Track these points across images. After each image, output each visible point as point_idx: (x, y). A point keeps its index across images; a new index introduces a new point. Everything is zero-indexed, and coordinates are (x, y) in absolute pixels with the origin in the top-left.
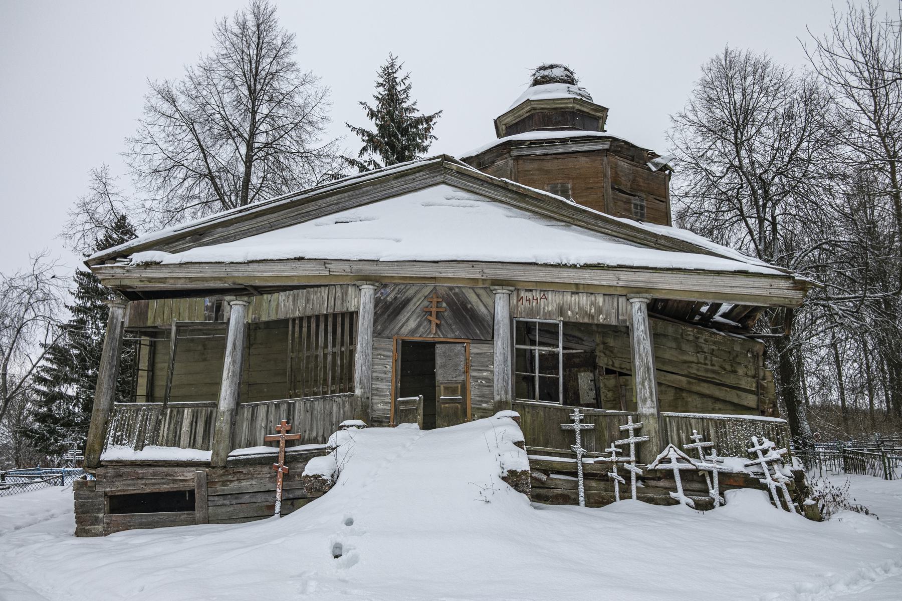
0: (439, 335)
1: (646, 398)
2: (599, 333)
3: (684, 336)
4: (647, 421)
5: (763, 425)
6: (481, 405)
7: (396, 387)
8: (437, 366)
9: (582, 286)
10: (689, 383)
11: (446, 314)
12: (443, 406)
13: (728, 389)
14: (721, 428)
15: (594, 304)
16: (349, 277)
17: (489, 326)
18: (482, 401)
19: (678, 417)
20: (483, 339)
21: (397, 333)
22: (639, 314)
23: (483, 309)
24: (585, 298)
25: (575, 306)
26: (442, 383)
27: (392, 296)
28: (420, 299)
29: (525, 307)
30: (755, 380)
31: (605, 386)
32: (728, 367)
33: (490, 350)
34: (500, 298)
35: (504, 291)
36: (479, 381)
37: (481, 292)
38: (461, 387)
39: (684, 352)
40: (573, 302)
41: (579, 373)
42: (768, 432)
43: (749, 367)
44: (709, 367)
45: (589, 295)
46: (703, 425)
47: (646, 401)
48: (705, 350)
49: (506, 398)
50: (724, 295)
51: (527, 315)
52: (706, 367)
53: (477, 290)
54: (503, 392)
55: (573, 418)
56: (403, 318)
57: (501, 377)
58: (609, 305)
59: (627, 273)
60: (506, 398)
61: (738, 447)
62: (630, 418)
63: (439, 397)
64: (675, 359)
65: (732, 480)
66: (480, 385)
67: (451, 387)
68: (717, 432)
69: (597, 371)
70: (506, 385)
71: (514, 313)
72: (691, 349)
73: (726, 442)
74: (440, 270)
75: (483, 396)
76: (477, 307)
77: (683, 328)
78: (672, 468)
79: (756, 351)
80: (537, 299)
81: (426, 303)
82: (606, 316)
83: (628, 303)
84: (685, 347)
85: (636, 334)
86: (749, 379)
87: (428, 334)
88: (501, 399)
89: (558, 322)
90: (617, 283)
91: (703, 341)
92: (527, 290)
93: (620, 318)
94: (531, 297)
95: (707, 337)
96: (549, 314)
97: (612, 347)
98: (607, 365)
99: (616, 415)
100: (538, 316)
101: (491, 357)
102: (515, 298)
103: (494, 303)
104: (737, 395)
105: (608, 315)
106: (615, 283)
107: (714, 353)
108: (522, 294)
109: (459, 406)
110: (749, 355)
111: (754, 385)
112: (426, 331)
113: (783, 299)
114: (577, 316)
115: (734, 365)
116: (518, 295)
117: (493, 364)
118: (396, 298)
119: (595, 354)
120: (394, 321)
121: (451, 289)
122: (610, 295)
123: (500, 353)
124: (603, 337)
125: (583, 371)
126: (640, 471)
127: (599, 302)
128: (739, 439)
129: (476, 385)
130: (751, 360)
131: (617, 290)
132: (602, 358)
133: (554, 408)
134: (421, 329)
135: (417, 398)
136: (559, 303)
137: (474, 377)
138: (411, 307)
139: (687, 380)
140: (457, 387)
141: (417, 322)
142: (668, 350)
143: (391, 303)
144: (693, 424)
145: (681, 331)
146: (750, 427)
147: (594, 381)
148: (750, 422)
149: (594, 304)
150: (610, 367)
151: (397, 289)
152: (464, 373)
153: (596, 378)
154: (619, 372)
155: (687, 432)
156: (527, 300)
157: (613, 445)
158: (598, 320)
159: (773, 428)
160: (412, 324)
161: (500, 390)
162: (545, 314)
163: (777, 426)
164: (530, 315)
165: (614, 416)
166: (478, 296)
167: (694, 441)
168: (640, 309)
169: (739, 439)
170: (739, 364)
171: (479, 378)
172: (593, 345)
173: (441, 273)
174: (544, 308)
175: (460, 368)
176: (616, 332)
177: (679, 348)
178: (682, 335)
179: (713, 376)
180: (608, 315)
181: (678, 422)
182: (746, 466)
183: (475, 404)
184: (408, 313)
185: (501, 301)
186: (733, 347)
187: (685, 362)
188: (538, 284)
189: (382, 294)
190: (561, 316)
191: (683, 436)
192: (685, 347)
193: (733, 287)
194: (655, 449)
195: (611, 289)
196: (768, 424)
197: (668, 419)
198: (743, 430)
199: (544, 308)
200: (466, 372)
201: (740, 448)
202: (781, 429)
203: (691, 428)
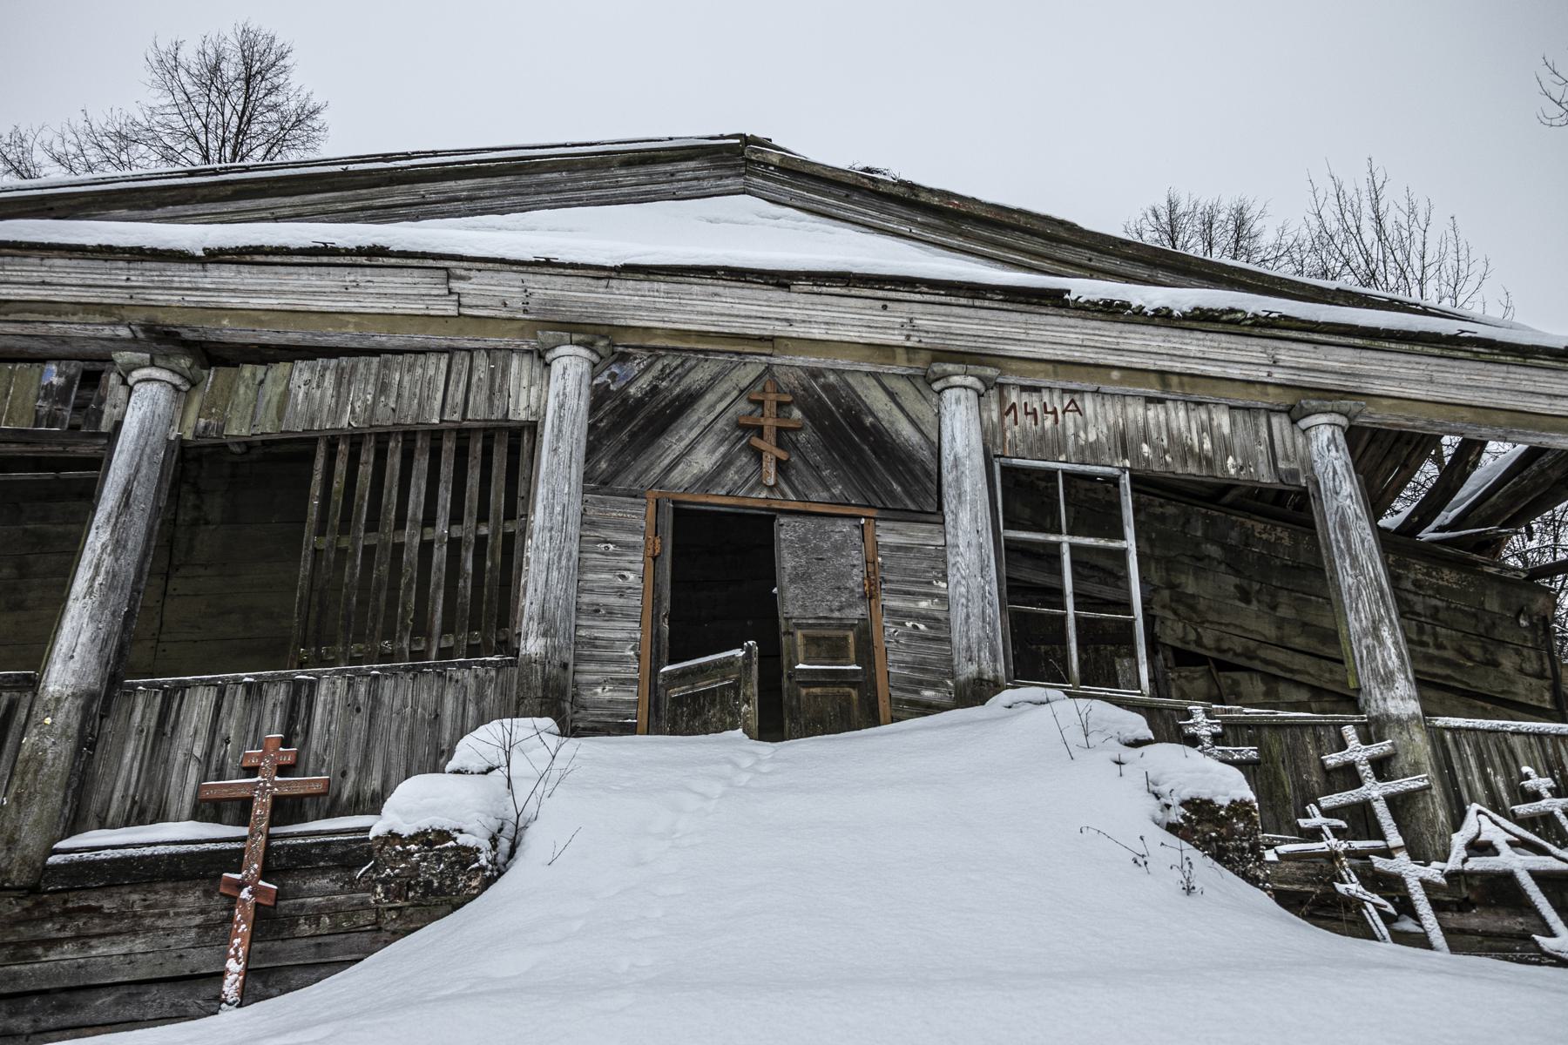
0: (783, 494)
1: (1392, 673)
4: (1405, 736)
6: (917, 692)
7: (656, 636)
8: (784, 577)
9: (1175, 380)
11: (802, 437)
12: (804, 691)
13: (1489, 706)
15: (1206, 428)
16: (516, 325)
17: (927, 474)
18: (920, 683)
19: (1474, 730)
20: (912, 506)
21: (658, 484)
22: (1333, 453)
23: (906, 430)
24: (1182, 414)
25: (1160, 433)
26: (798, 626)
27: (644, 383)
28: (726, 395)
29: (1024, 431)
30: (1546, 683)
32: (1476, 652)
33: (934, 539)
34: (958, 401)
35: (970, 381)
36: (909, 624)
37: (900, 386)
38: (858, 639)
40: (1152, 422)
41: (1117, 660)
43: (1525, 652)
44: (1432, 651)
45: (1192, 406)
46: (1544, 751)
47: (1394, 681)
48: (1419, 608)
49: (995, 670)
50: (1534, 418)
51: (1030, 449)
52: (1423, 649)
53: (886, 382)
54: (985, 654)
55: (1192, 730)
56: (675, 442)
57: (975, 610)
58: (1248, 435)
59: (1295, 346)
60: (995, 670)
62: (1349, 732)
63: (792, 664)
66: (910, 636)
67: (824, 638)
69: (1161, 656)
70: (991, 635)
71: (994, 444)
74: (790, 313)
75: (920, 666)
76: (892, 423)
78: (1508, 867)
79: (1537, 614)
80: (1055, 412)
81: (743, 406)
82: (1244, 459)
83: (1297, 431)
85: (1330, 506)
86: (1534, 681)
87: (752, 489)
88: (980, 672)
89: (1116, 472)
90: (1269, 375)
91: (1409, 586)
92: (1024, 388)
93: (1282, 465)
94: (1037, 406)
95: (1420, 576)
97: (1193, 596)
98: (1184, 640)
99: (1307, 725)
100: (1060, 454)
101: (940, 561)
102: (995, 406)
103: (938, 415)
105: (1248, 459)
106: (1261, 374)
107: (1441, 615)
108: (1013, 397)
109: (854, 693)
110: (1523, 623)
111: (1547, 696)
112: (747, 481)
114: (1168, 458)
116: (1002, 400)
117: (945, 578)
118: (654, 390)
120: (650, 450)
121: (815, 374)
122: (1248, 409)
123: (969, 544)
124: (1167, 570)
126: (1434, 872)
127: (1219, 426)
129: (902, 635)
130: (1529, 636)
131: (1268, 395)
132: (1169, 623)
134: (731, 475)
135: (739, 653)
136: (1116, 423)
137: (894, 612)
138: (700, 414)
140: (845, 638)
141: (718, 455)
143: (640, 403)
149: (1206, 428)
150: (1193, 648)
151: (659, 366)
152: (864, 597)
154: (1215, 660)
155: (1508, 774)
156: (1027, 414)
157: (1312, 808)
158: (1225, 469)
160: (704, 460)
161: (975, 647)
162: (1081, 450)
164: (1041, 450)
165: (1302, 726)
166: (892, 396)
167: (1536, 796)
168: (1333, 440)
170: (1502, 643)
171: (909, 615)
173: (789, 322)
174: (1076, 435)
175: (850, 584)
176: (1199, 559)
179: (1449, 672)
180: (1248, 459)
181: (1477, 744)
183: (899, 689)
184: (691, 429)
185: (962, 407)
186: (1482, 603)
188: (1060, 368)
189: (613, 376)
190: (1125, 456)
191: (1500, 782)
193: (1556, 396)
194: (1442, 815)
197: (1448, 736)
199: (1076, 435)
200: (869, 596)
203: (1516, 761)
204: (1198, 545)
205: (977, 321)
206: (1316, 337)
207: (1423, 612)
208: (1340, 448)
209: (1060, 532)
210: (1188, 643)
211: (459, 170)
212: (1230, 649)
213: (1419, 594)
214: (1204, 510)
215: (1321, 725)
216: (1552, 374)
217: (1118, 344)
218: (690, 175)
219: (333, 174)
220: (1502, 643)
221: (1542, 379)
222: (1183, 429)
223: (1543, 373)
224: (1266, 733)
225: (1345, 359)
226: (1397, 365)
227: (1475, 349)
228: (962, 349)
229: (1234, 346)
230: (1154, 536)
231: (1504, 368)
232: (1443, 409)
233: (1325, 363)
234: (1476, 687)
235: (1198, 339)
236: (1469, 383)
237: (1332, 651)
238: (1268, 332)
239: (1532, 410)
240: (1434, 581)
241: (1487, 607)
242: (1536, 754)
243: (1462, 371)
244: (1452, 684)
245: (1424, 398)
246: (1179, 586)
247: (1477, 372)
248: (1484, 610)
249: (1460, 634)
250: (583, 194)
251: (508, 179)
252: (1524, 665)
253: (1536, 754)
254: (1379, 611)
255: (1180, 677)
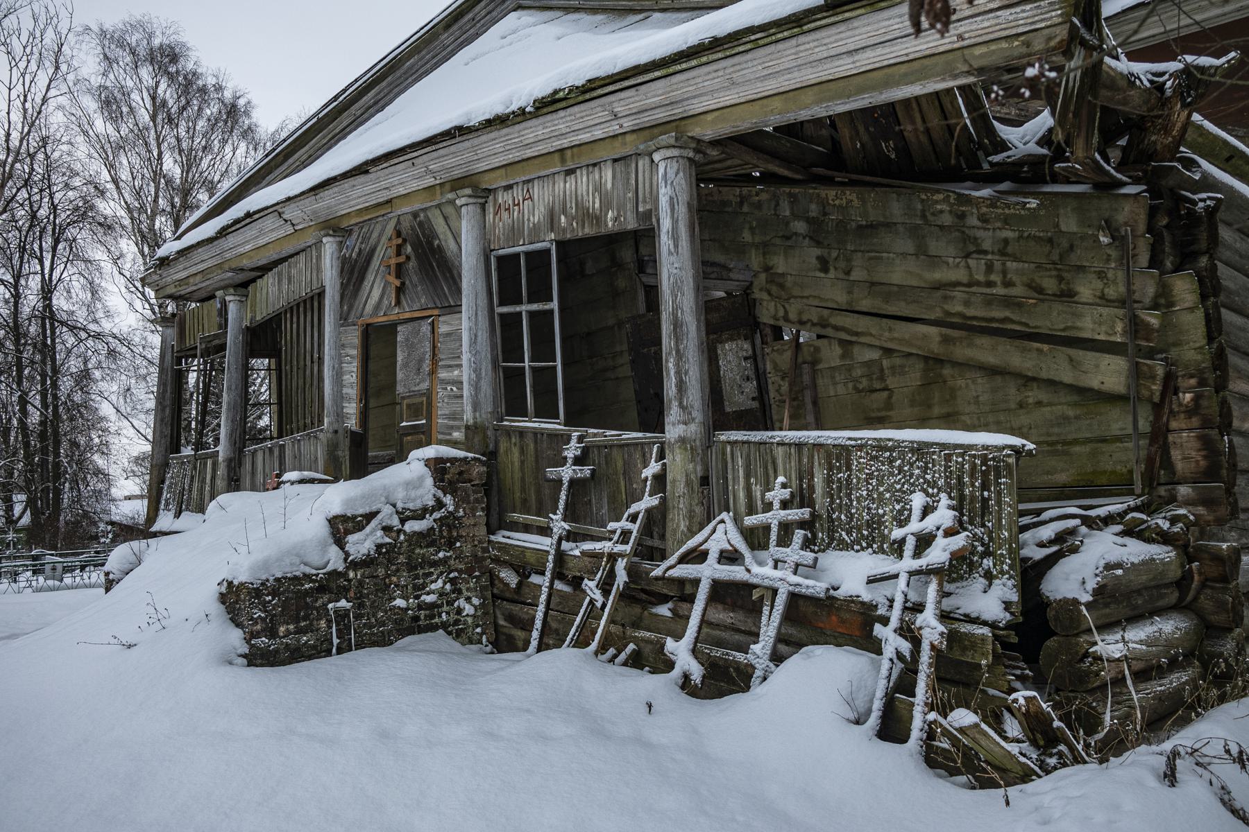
2: (757, 246)
3: (930, 218)
5: (948, 458)
10: (946, 340)
13: (1045, 347)
14: (839, 470)
15: (599, 188)
16: (312, 229)
18: (452, 427)
19: (748, 442)
31: (776, 367)
32: (1050, 284)
39: (934, 261)
41: (719, 346)
42: (960, 479)
43: (1110, 275)
44: (999, 290)
45: (591, 169)
48: (986, 245)
49: (475, 418)
50: (841, 84)
52: (988, 291)
61: (875, 524)
64: (914, 283)
65: (834, 618)
66: (449, 396)
68: (828, 481)
72: (951, 250)
73: (850, 506)
74: (383, 184)
76: (446, 241)
77: (924, 197)
79: (1126, 224)
84: (937, 246)
90: (621, 126)
93: (641, 209)
95: (984, 210)
96: (536, 232)
97: (783, 274)
99: (637, 444)
104: (1071, 360)
106: (614, 128)
107: (1009, 250)
111: (1119, 327)
113: (1004, 45)
114: (575, 224)
115: (1065, 275)
119: (753, 296)
124: (764, 254)
125: (727, 340)
128: (881, 501)
132: (765, 303)
133: (549, 435)
138: (375, 263)
139: (941, 335)
142: (898, 261)
143: (356, 261)
144: (780, 462)
145: (919, 206)
146: (911, 465)
147: (754, 358)
148: (912, 450)
149: (599, 188)
153: (758, 352)
159: (973, 466)
163: (985, 460)
165: (636, 445)
169: (881, 501)
170: (1081, 269)
172: (747, 276)
176: (788, 238)
177: (921, 251)
178: (924, 216)
179: (1007, 314)
181: (748, 456)
182: (871, 581)
183: (443, 433)
186: (1057, 225)
187: (938, 286)
192: (937, 246)
195: (617, 143)
196: (962, 455)
198: (892, 474)
199: (529, 220)
200: (433, 372)
201: (879, 529)
202: (997, 469)
203: (775, 471)
204: (787, 224)
205: (451, 156)
206: (626, 83)
207: (990, 249)
208: (669, 182)
209: (520, 302)
210: (777, 320)
211: (365, 87)
212: (809, 320)
213: (989, 229)
214: (787, 190)
215: (645, 443)
216: (842, 27)
217: (521, 141)
218: (483, 13)
219: (314, 124)
220: (1081, 269)
221: (832, 39)
222: (585, 193)
223: (833, 30)
224: (615, 451)
225: (660, 92)
226: (700, 80)
227: (753, 38)
228: (460, 176)
229: (584, 114)
230: (754, 224)
231: (793, 42)
232: (757, 105)
233: (647, 101)
234: (1036, 327)
235: (562, 118)
236: (766, 72)
237: (894, 309)
238: (595, 94)
239: (837, 76)
240: (1000, 211)
241: (1064, 228)
242: (793, 464)
243: (755, 63)
244: (1010, 326)
245: (738, 101)
246: (771, 268)
247: (768, 58)
248: (1061, 231)
249: (1032, 266)
250: (428, 66)
251: (390, 78)
252: (1106, 290)
253: (793, 464)
254: (670, 343)
255: (773, 350)
